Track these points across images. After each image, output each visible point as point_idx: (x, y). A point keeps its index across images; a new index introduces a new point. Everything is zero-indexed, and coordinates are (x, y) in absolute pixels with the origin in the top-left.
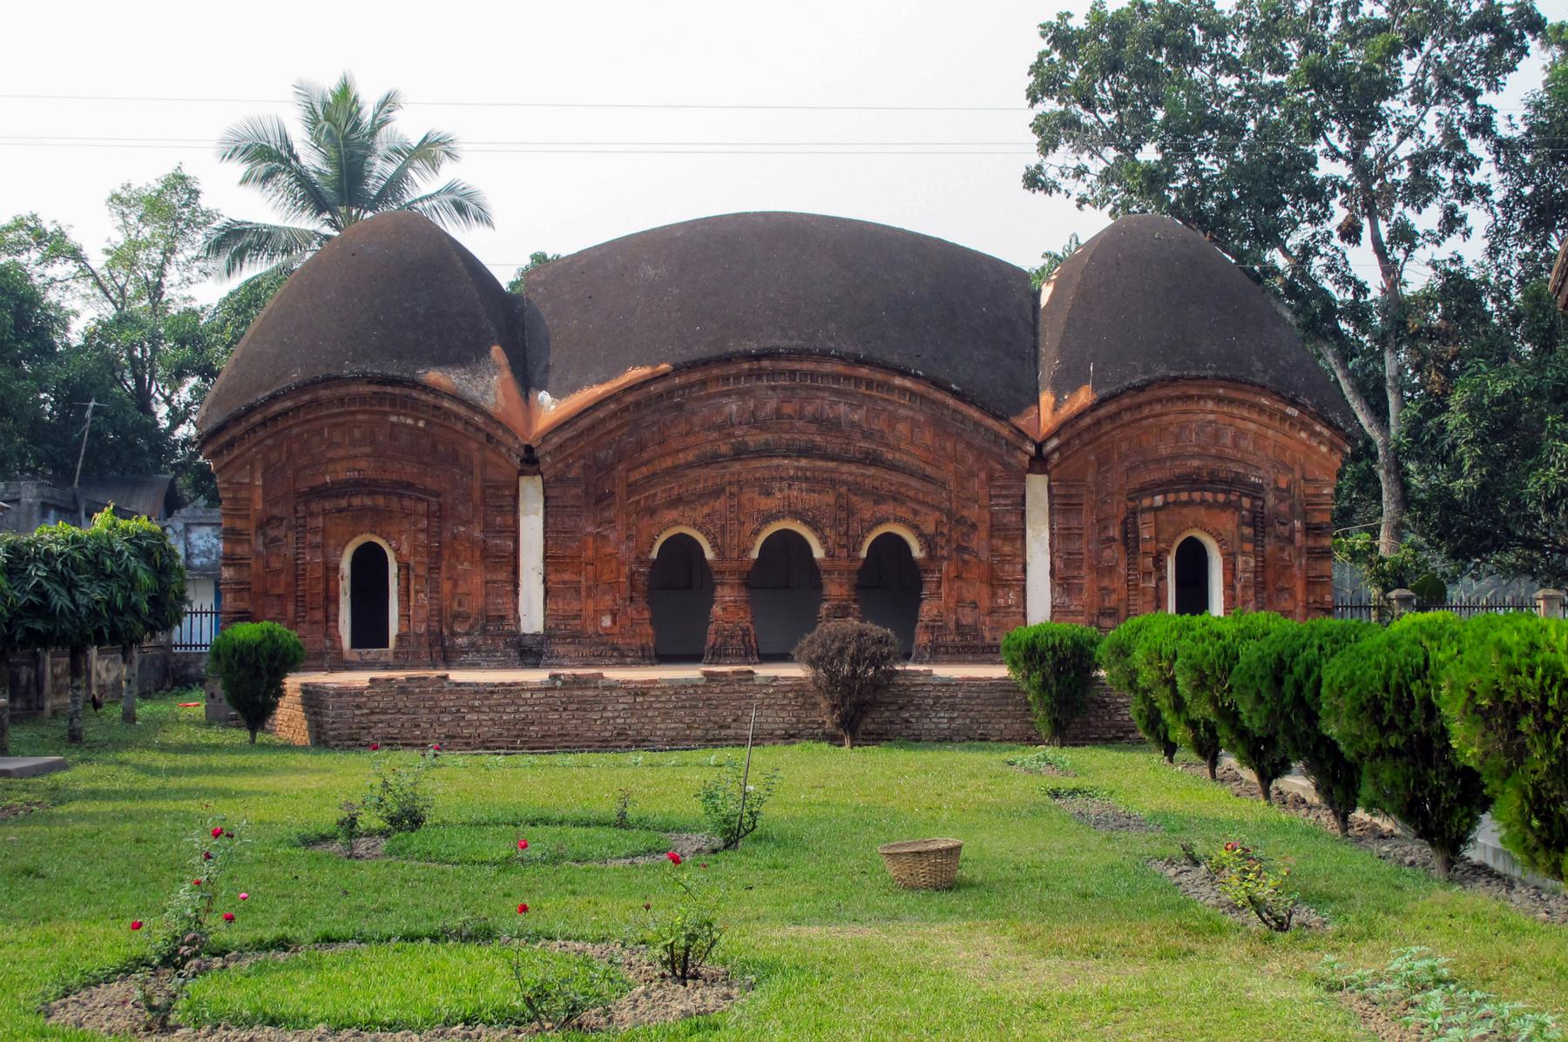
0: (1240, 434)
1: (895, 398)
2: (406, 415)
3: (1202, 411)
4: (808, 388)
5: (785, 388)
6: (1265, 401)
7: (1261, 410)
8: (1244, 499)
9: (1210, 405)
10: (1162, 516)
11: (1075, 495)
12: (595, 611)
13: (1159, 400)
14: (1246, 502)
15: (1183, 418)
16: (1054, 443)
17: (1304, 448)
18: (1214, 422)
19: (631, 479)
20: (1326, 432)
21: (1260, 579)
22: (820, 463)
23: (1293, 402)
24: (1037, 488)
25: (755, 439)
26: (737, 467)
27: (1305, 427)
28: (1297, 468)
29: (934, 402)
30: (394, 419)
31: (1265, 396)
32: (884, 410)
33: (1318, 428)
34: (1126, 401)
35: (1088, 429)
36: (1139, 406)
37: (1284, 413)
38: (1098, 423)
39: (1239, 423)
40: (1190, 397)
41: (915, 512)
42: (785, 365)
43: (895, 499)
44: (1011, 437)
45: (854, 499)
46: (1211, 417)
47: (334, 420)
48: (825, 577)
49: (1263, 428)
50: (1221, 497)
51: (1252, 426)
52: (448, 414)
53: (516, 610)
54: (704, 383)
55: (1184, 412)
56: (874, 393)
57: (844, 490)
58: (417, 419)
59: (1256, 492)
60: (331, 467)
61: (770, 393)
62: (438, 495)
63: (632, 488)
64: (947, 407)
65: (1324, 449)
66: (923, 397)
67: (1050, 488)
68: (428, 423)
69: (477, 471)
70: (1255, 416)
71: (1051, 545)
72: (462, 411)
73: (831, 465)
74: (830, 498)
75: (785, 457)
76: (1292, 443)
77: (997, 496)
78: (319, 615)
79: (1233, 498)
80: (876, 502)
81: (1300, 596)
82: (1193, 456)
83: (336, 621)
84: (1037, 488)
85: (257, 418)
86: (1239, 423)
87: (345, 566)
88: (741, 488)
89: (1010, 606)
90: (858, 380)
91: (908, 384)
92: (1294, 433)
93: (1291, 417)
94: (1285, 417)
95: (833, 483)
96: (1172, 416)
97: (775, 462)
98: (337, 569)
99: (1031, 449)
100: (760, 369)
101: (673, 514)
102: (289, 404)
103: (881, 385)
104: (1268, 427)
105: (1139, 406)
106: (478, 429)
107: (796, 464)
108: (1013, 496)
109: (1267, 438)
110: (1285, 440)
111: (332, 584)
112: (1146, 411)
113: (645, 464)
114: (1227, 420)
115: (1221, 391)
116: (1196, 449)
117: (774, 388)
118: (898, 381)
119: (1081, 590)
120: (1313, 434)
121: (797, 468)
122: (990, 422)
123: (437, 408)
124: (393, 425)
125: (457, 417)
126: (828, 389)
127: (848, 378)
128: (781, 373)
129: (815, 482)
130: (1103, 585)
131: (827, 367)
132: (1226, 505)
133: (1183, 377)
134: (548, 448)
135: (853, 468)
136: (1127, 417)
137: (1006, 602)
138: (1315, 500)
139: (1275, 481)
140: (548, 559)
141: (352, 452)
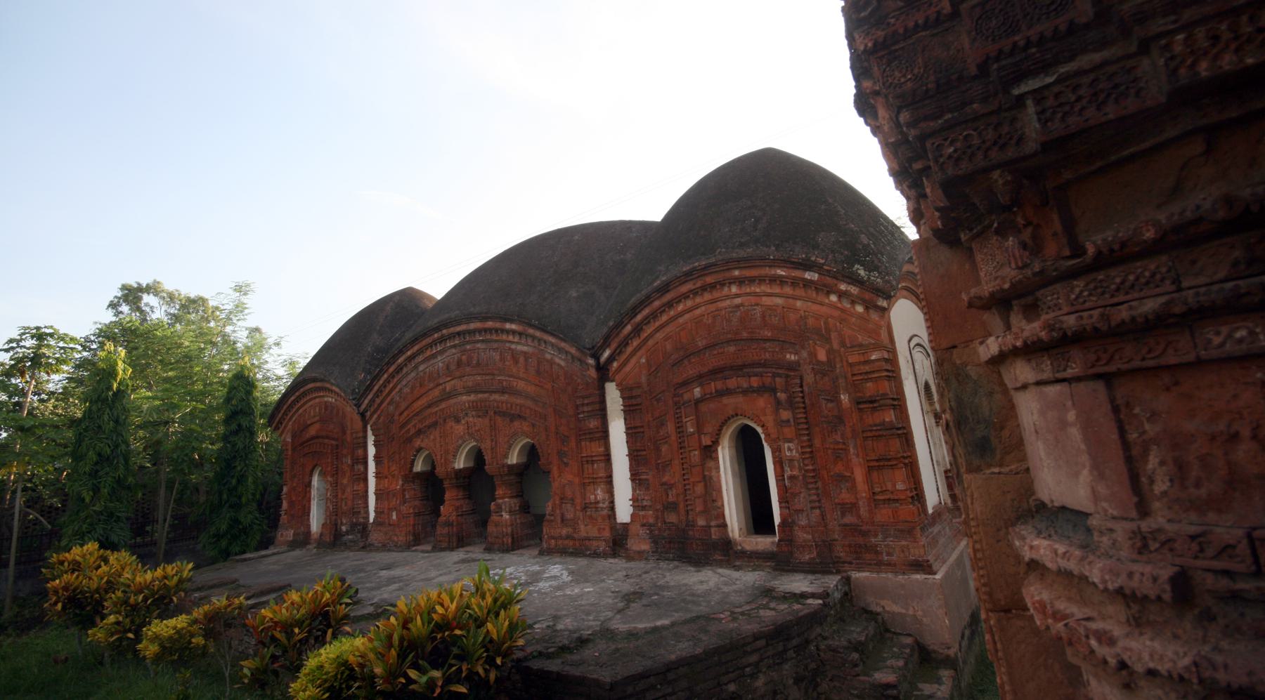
1: (511, 338)
3: (728, 297)
6: (781, 272)
7: (781, 281)
8: (778, 380)
9: (734, 289)
11: (635, 397)
12: (389, 509)
15: (712, 307)
16: (607, 354)
17: (837, 313)
18: (742, 305)
20: (854, 290)
21: (810, 467)
22: (480, 396)
23: (807, 266)
25: (448, 387)
26: (443, 405)
28: (834, 335)
31: (779, 267)
32: (510, 349)
33: (843, 287)
34: (657, 303)
36: (670, 305)
37: (804, 280)
39: (767, 301)
40: (713, 287)
42: (452, 330)
45: (499, 419)
46: (738, 301)
49: (791, 301)
51: (779, 301)
61: (454, 351)
70: (777, 290)
73: (486, 395)
76: (824, 310)
77: (583, 405)
79: (768, 380)
82: (728, 342)
83: (309, 515)
86: (767, 301)
88: (445, 420)
89: (598, 502)
92: (821, 298)
93: (811, 281)
94: (807, 284)
96: (703, 308)
99: (591, 361)
100: (443, 336)
104: (795, 298)
107: (469, 398)
108: (592, 403)
109: (796, 310)
110: (815, 307)
114: (753, 300)
115: (737, 273)
116: (729, 336)
117: (454, 346)
118: (508, 326)
121: (469, 402)
130: (664, 480)
132: (763, 390)
133: (694, 269)
135: (496, 397)
137: (596, 498)
138: (867, 368)
139: (813, 355)
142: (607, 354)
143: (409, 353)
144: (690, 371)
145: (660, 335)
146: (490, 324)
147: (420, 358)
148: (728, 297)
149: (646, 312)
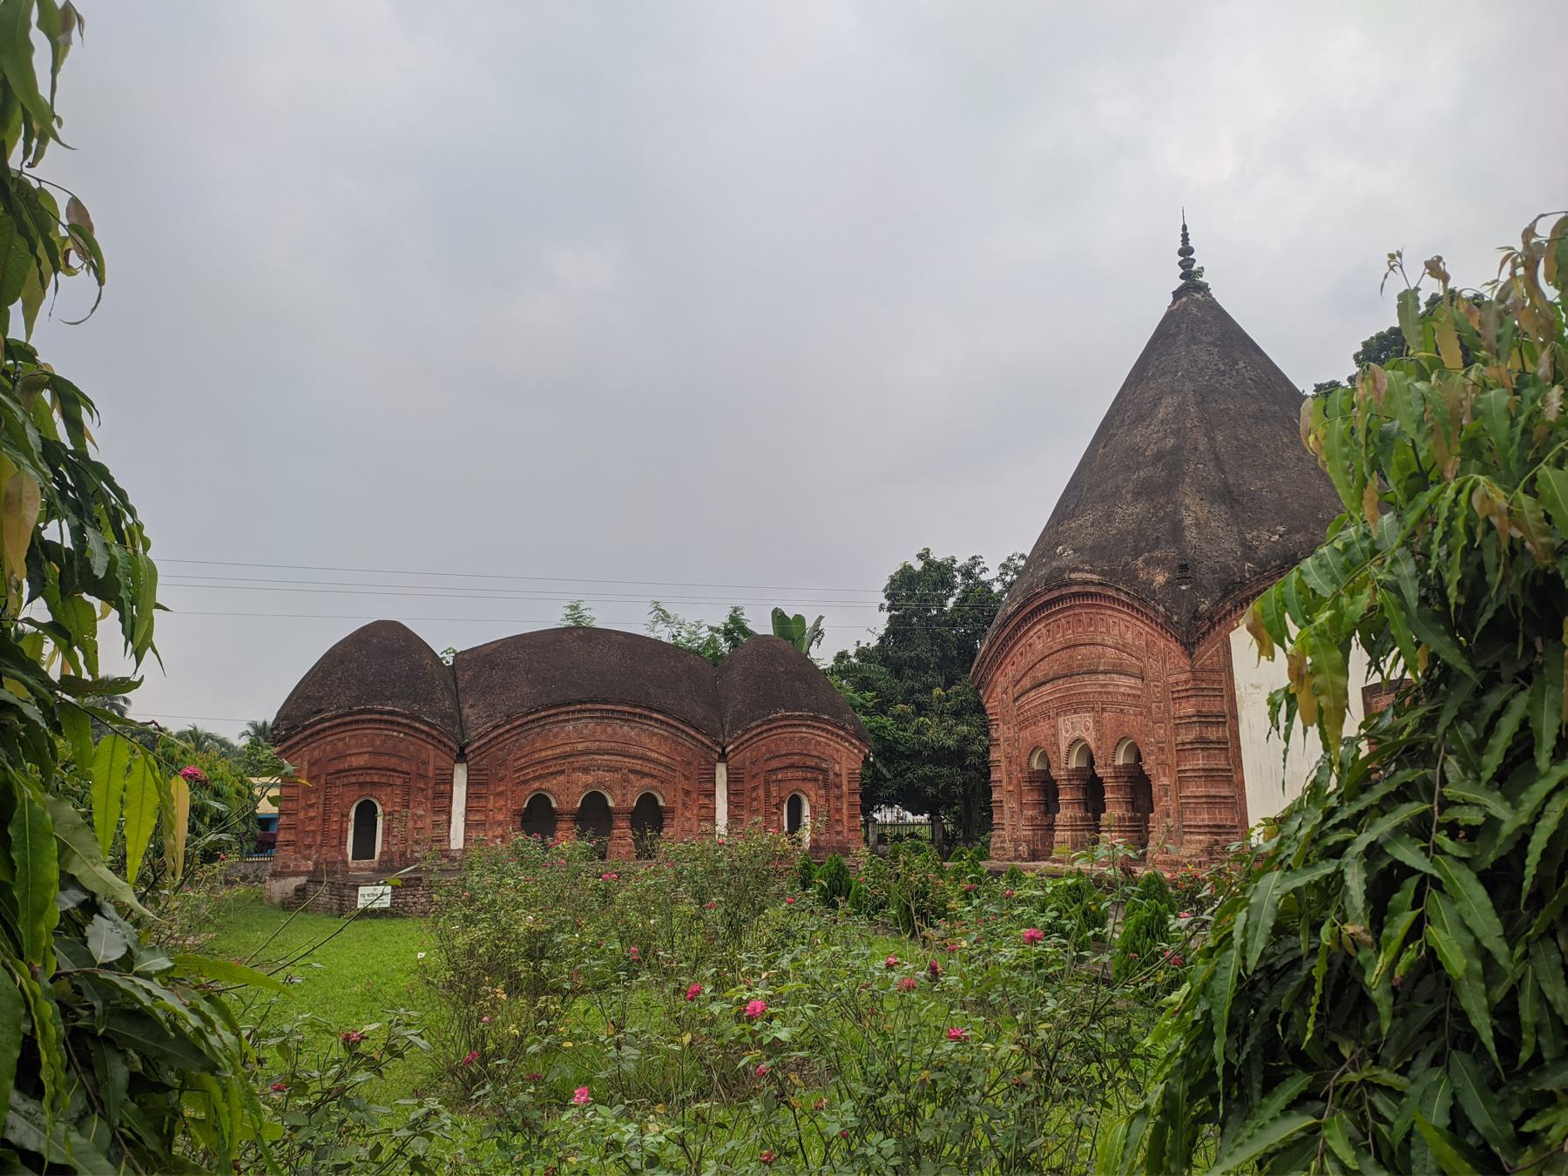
0: (819, 743)
2: (394, 731)
3: (801, 732)
4: (608, 718)
5: (597, 717)
7: (828, 731)
9: (804, 729)
10: (782, 784)
13: (780, 727)
14: (821, 777)
15: (791, 735)
16: (731, 747)
19: (516, 764)
20: (857, 743)
23: (843, 728)
24: (721, 771)
25: (580, 747)
27: (847, 741)
29: (672, 726)
30: (386, 732)
33: (854, 741)
35: (747, 741)
36: (771, 729)
38: (751, 738)
41: (662, 782)
43: (652, 776)
44: (710, 745)
45: (631, 776)
47: (352, 733)
48: (614, 817)
50: (809, 775)
52: (417, 729)
53: (449, 836)
54: (556, 715)
55: (791, 732)
56: (643, 721)
57: (626, 771)
58: (400, 732)
59: (825, 771)
60: (348, 758)
62: (408, 774)
63: (516, 771)
64: (678, 729)
65: (856, 751)
66: (667, 724)
67: (727, 770)
68: (405, 734)
69: (432, 761)
71: (728, 798)
72: (426, 728)
74: (618, 776)
75: (596, 754)
76: (841, 748)
78: (335, 842)
80: (642, 777)
81: (846, 824)
82: (796, 754)
84: (721, 771)
85: (308, 732)
87: (352, 814)
90: (635, 714)
91: (660, 717)
94: (838, 736)
95: (618, 770)
97: (591, 757)
98: (347, 815)
99: (720, 750)
101: (536, 785)
102: (327, 724)
103: (646, 717)
105: (771, 729)
106: (434, 738)
107: (601, 757)
110: (838, 746)
111: (345, 824)
112: (774, 732)
113: (524, 757)
114: (812, 736)
118: (655, 715)
119: (742, 820)
120: (851, 744)
122: (699, 737)
123: (411, 727)
124: (386, 735)
125: (422, 732)
126: (617, 719)
127: (629, 713)
128: (596, 710)
129: (611, 769)
131: (620, 708)
134: (472, 748)
136: (765, 735)
140: (468, 810)
141: (361, 750)
142: (731, 747)
143: (543, 714)
144: (774, 764)
145: (761, 743)
146: (638, 710)
147: (552, 719)
148: (801, 732)
149: (759, 730)
